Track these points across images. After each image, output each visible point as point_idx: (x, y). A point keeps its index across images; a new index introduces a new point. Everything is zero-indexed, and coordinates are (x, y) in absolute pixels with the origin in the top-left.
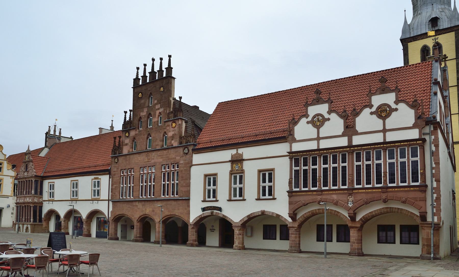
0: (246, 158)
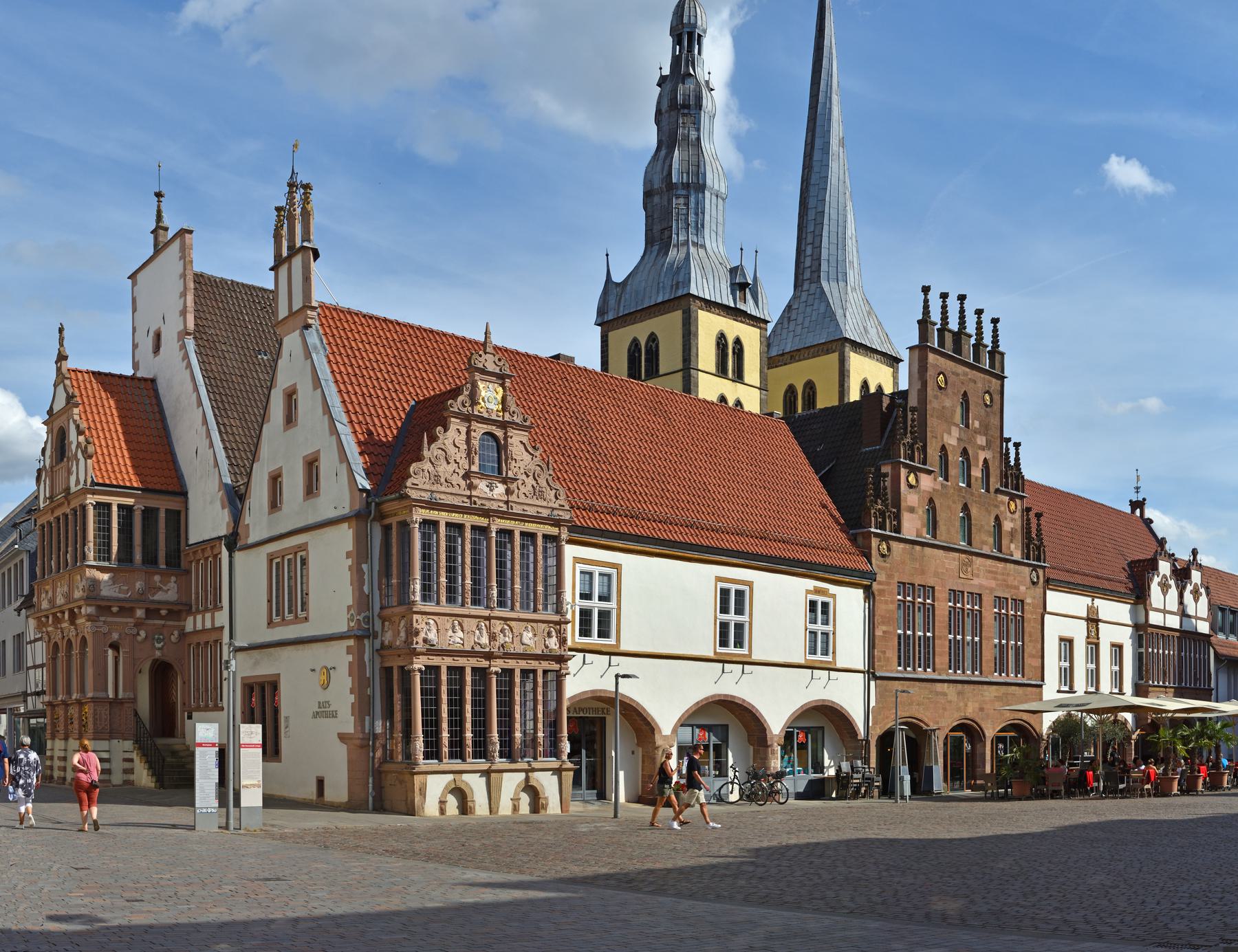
0: (1104, 619)
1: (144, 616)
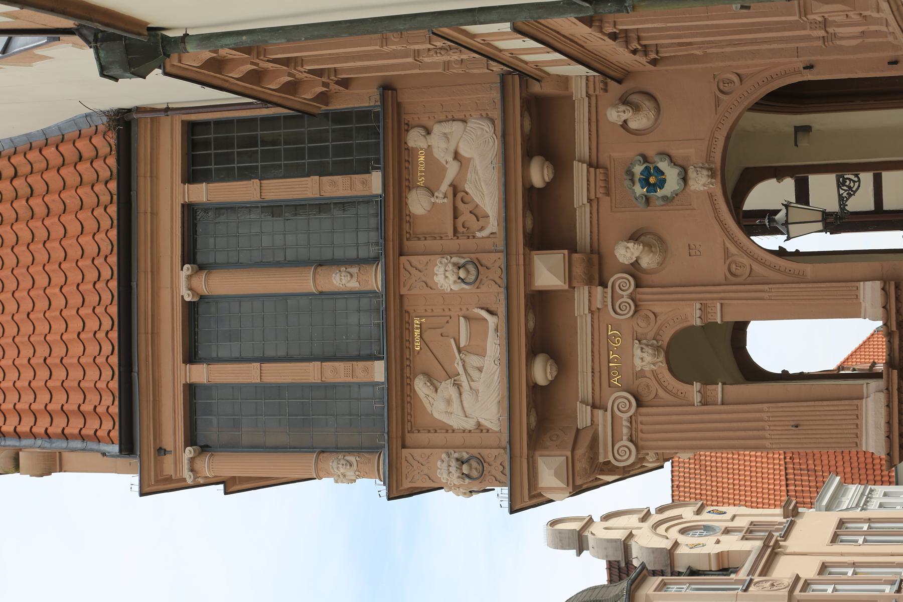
1: (557, 258)
